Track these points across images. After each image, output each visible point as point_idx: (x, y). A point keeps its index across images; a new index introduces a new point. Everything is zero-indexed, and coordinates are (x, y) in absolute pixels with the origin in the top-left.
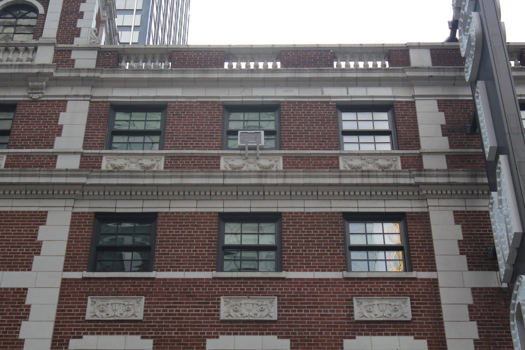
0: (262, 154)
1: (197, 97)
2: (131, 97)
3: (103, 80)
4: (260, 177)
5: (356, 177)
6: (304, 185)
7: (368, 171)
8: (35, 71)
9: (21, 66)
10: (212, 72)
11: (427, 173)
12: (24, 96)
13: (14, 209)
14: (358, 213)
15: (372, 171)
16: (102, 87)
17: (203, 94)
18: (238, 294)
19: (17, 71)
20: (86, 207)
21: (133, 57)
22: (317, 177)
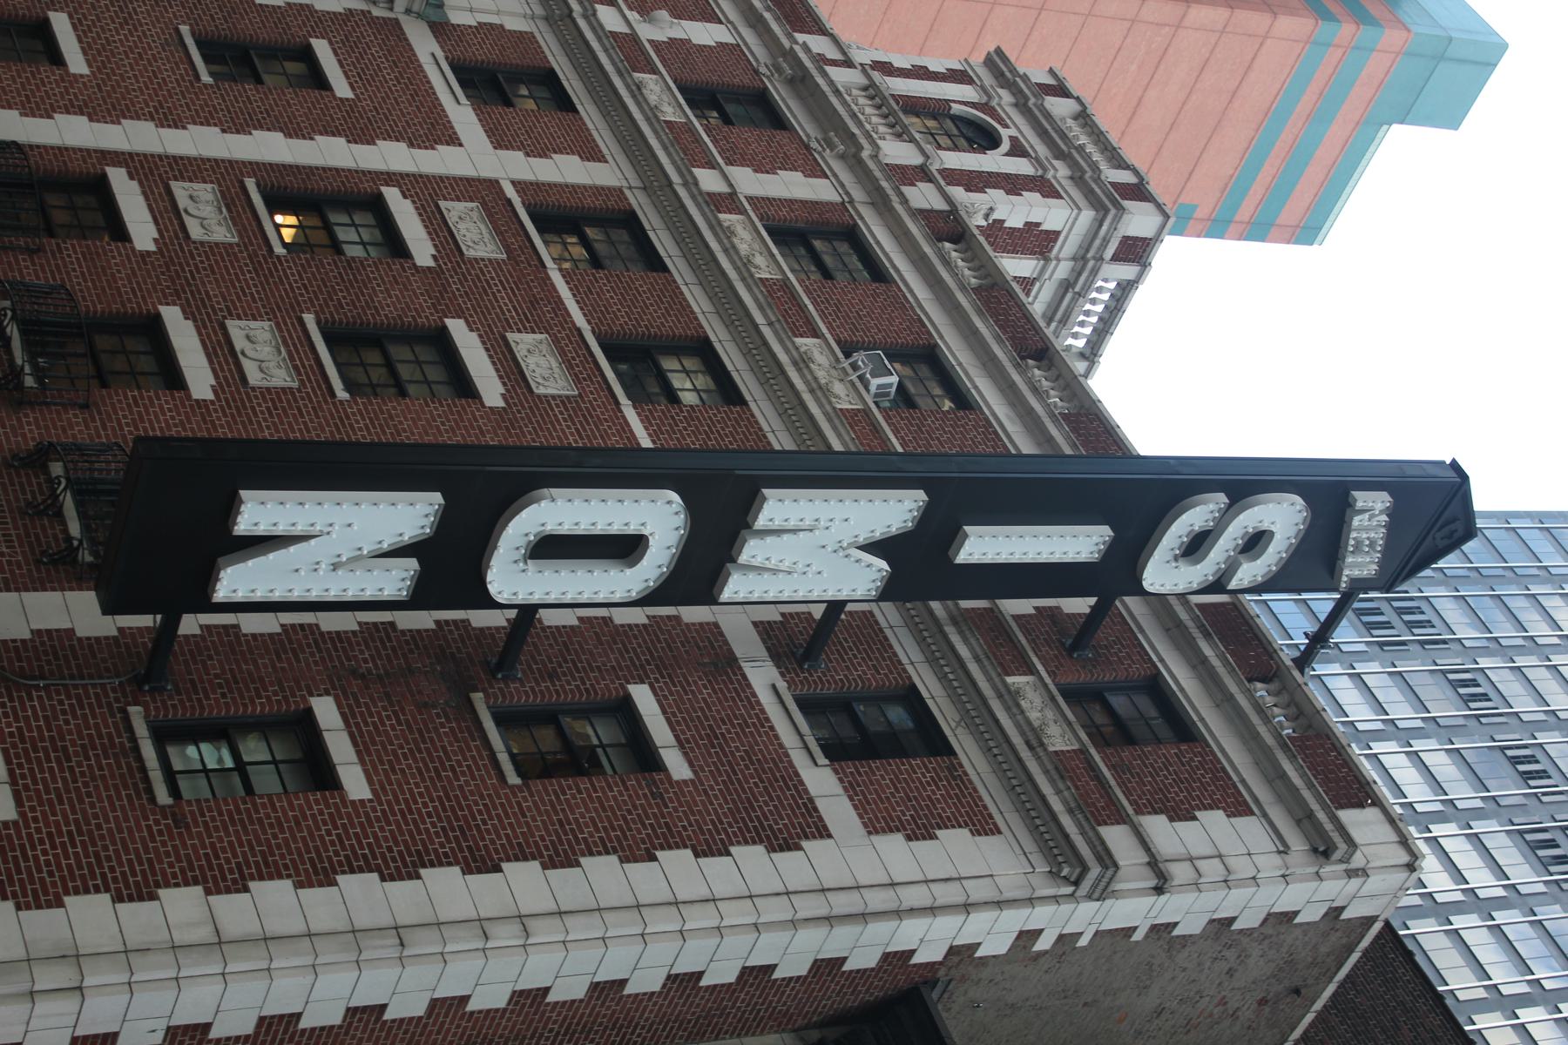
0: (852, 383)
1: (926, 314)
2: (878, 243)
3: (891, 210)
4: (795, 363)
5: (720, 242)
6: (811, 417)
7: (734, 247)
8: (855, 130)
9: (854, 116)
10: (985, 320)
11: (806, 371)
12: (808, 136)
13: (594, 133)
14: (727, 374)
15: (737, 252)
16: (880, 214)
17: (888, 249)
18: (490, 215)
19: (826, 88)
20: (638, 202)
21: (977, 263)
22: (835, 428)
